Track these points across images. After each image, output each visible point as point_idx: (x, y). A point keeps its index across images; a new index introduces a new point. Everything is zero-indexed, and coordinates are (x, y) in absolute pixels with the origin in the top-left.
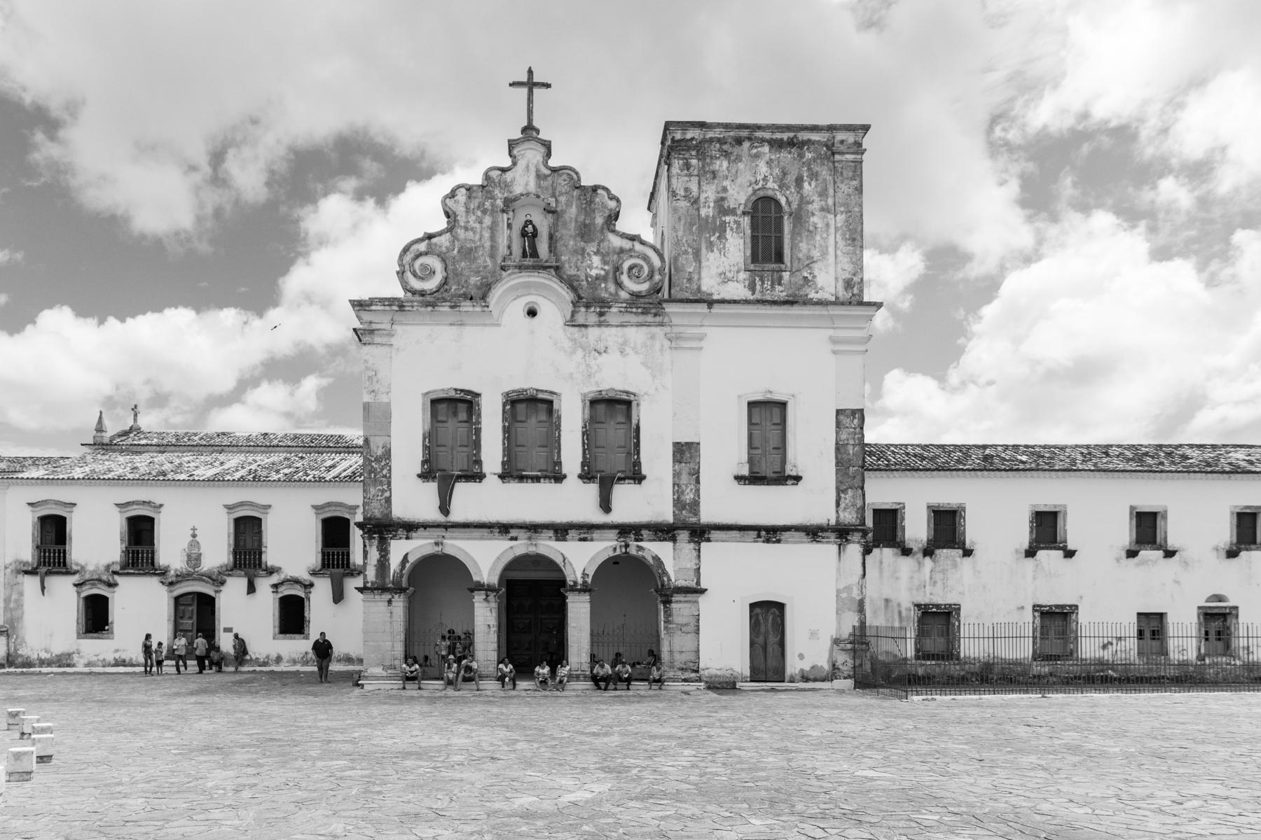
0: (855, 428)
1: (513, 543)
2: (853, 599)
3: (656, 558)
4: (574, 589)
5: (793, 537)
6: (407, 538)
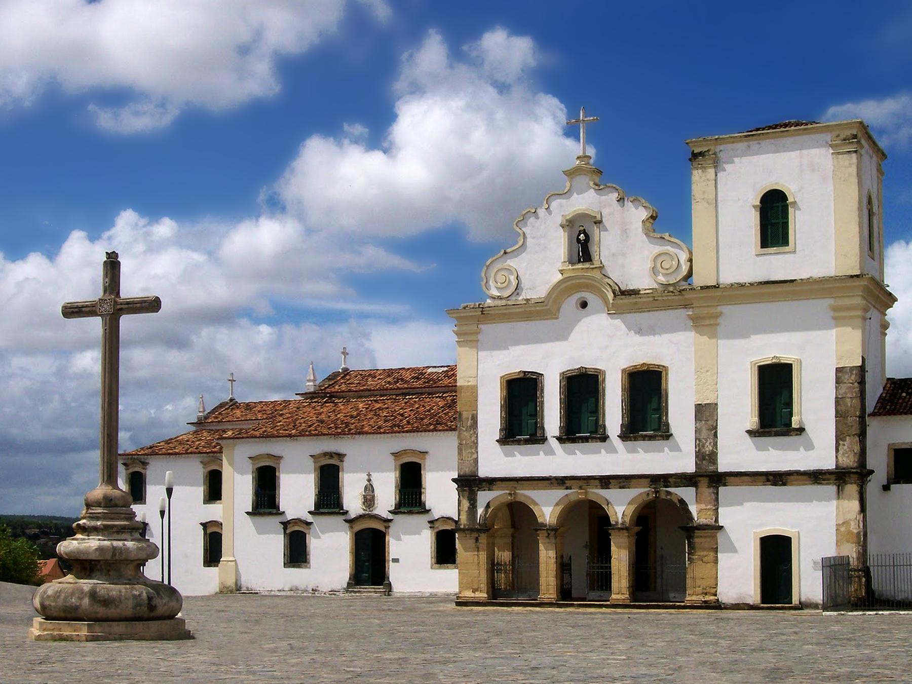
1: (569, 491)
2: (852, 533)
3: (682, 502)
4: (615, 527)
5: (796, 480)
6: (489, 490)
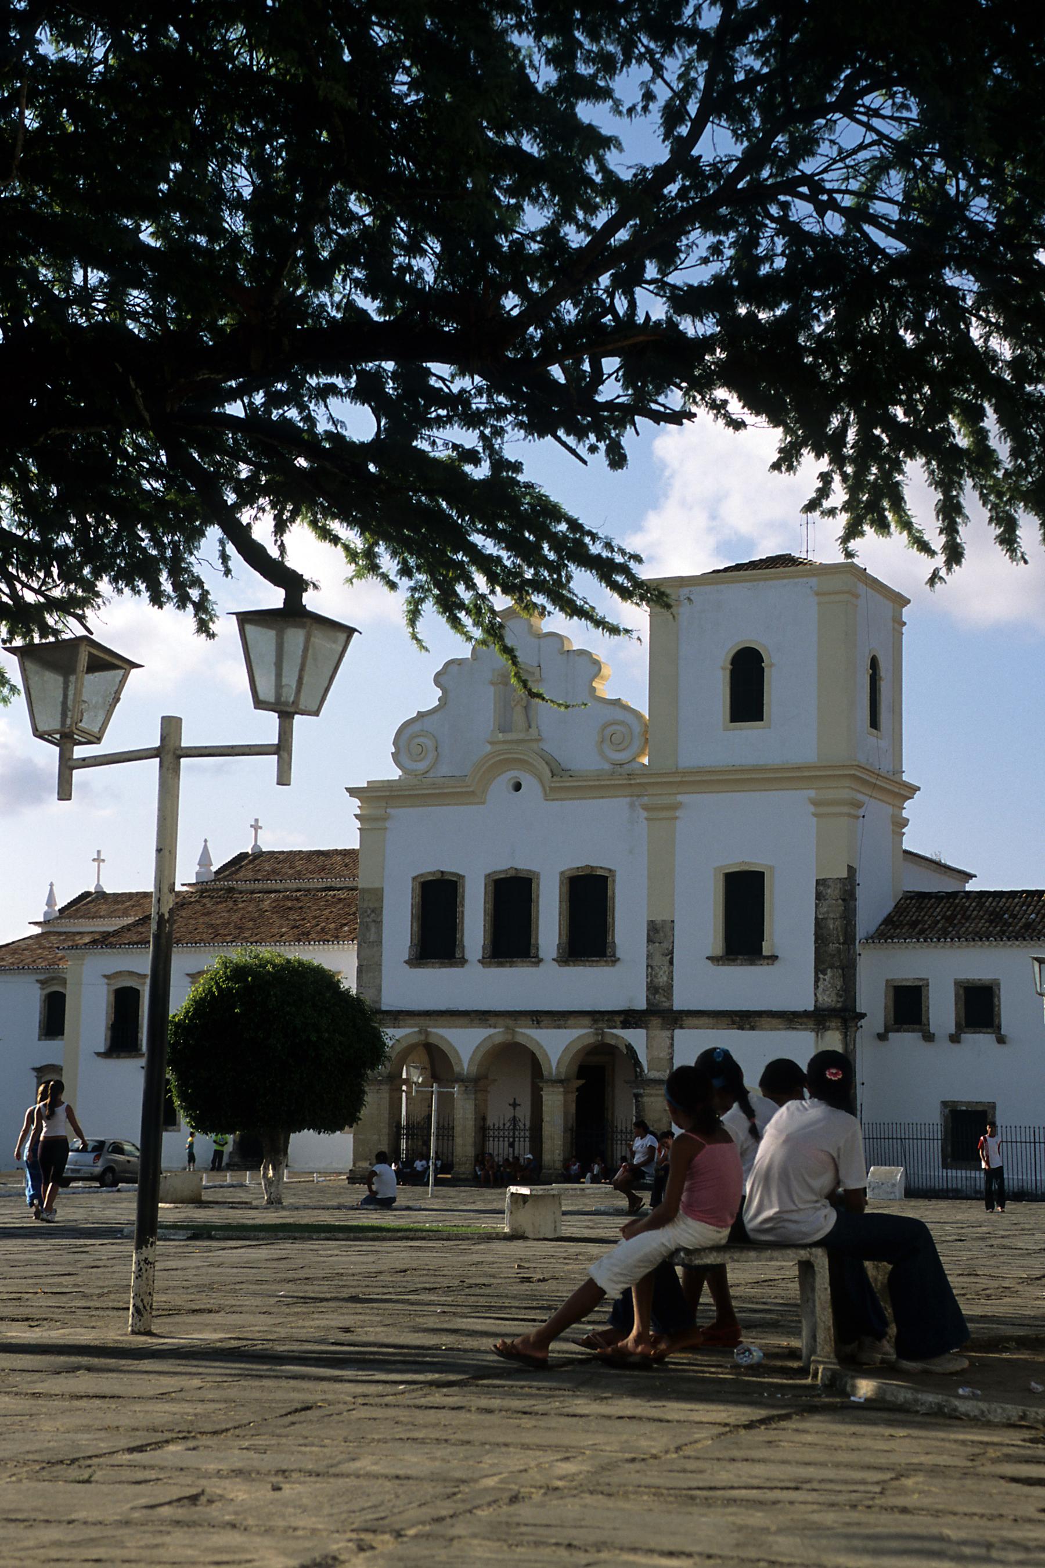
0: (837, 900)
3: (630, 1048)
